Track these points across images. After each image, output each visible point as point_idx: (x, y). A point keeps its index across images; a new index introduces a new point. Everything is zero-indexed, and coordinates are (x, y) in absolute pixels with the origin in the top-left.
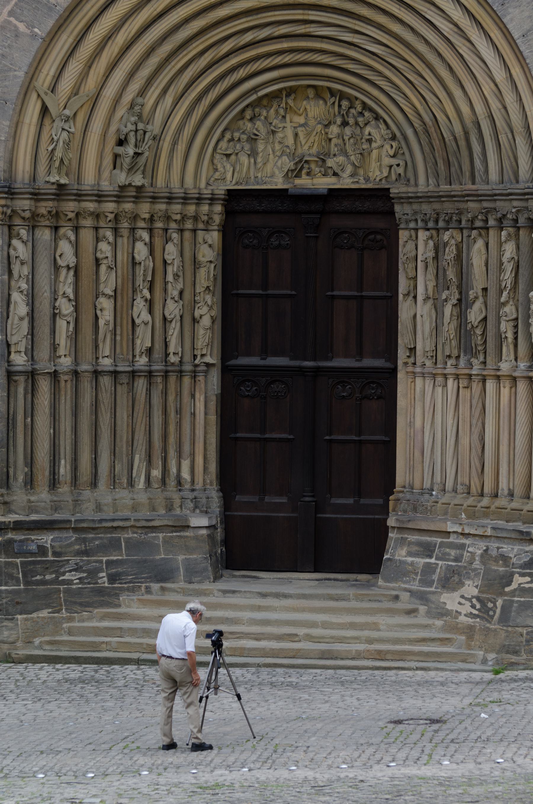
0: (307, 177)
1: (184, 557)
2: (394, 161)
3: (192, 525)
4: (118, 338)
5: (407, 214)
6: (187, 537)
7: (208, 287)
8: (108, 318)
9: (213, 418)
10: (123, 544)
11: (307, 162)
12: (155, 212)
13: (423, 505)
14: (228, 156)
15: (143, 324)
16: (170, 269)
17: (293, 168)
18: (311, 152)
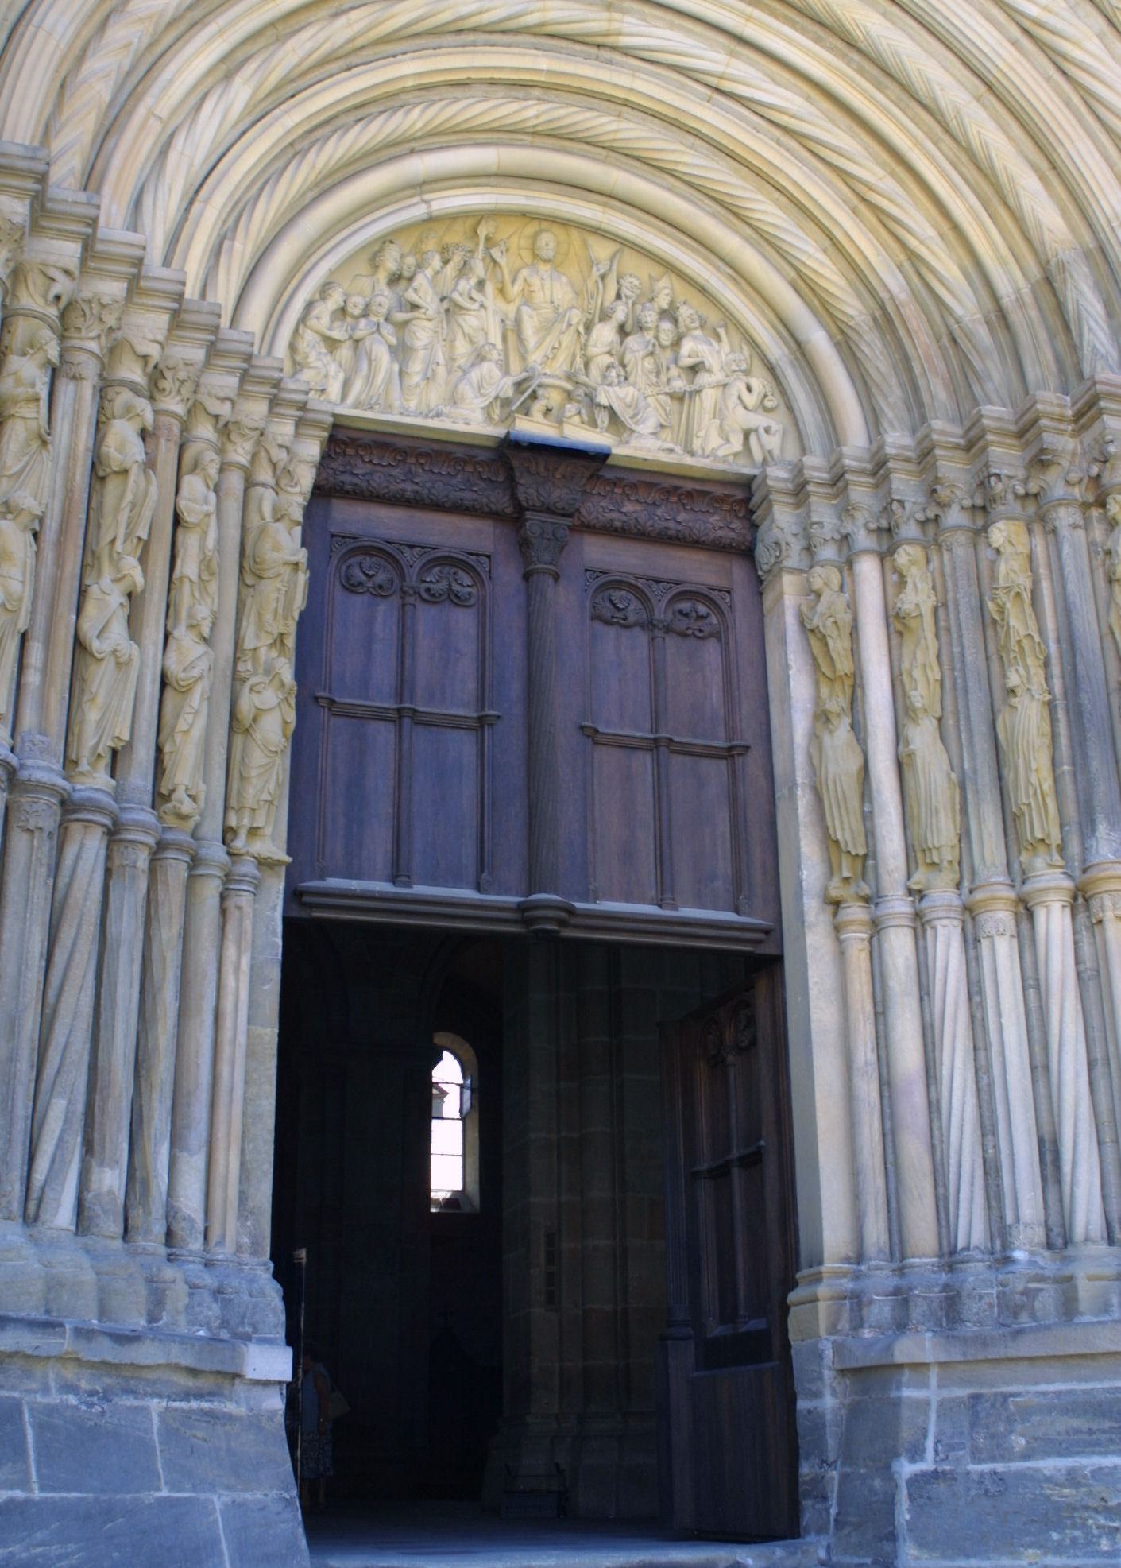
0: (545, 421)
1: (228, 1497)
2: (759, 420)
3: (250, 1375)
4: (33, 678)
5: (820, 524)
6: (230, 1418)
7: (282, 635)
8: (16, 587)
9: (270, 1034)
10: (30, 1433)
11: (540, 386)
12: (171, 364)
13: (981, 1297)
14: (332, 344)
15: (110, 663)
16: (190, 543)
17: (510, 393)
18: (548, 371)
